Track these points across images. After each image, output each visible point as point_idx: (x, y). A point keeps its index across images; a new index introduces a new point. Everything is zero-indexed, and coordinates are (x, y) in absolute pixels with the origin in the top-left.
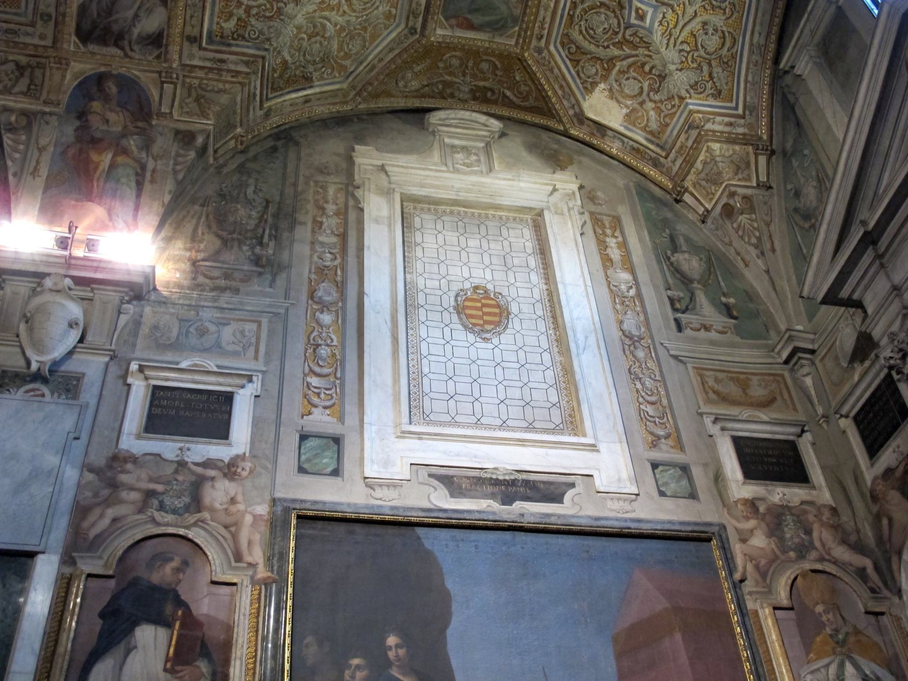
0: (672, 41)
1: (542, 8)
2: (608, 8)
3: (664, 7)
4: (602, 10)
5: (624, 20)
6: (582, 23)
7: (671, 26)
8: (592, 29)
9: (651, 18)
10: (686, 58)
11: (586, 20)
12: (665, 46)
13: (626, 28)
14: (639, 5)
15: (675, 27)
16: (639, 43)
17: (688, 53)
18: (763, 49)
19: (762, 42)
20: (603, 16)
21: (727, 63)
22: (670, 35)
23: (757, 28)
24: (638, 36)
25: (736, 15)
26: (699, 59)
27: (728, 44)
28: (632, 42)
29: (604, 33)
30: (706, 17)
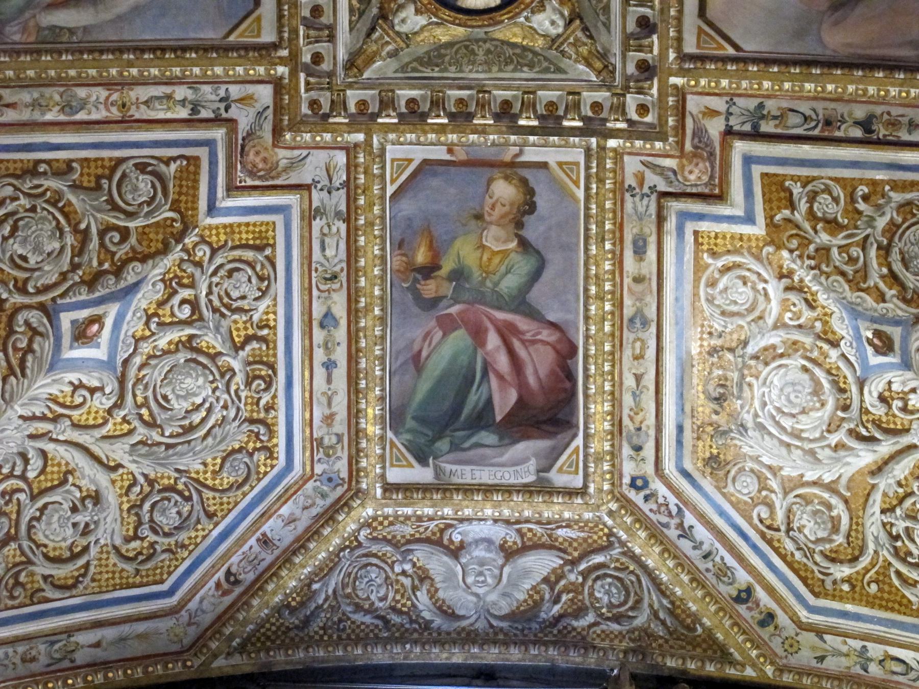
0: (44, 427)
1: (36, 95)
2: (80, 251)
3: (116, 385)
4: (70, 240)
5: (62, 296)
6: (24, 202)
7: (75, 414)
8: (15, 229)
9: (83, 360)
10: (11, 475)
11: (33, 209)
12: (27, 412)
13: (42, 307)
14: (109, 322)
15: (76, 426)
16: (16, 349)
17: (23, 477)
18: (66, 664)
19: (81, 657)
20: (57, 245)
21: (17, 583)
22: (56, 419)
23: (110, 633)
24: (31, 341)
25: (130, 568)
26: (12, 508)
27: (61, 572)
28: (11, 332)
29: (12, 259)
30: (111, 497)
